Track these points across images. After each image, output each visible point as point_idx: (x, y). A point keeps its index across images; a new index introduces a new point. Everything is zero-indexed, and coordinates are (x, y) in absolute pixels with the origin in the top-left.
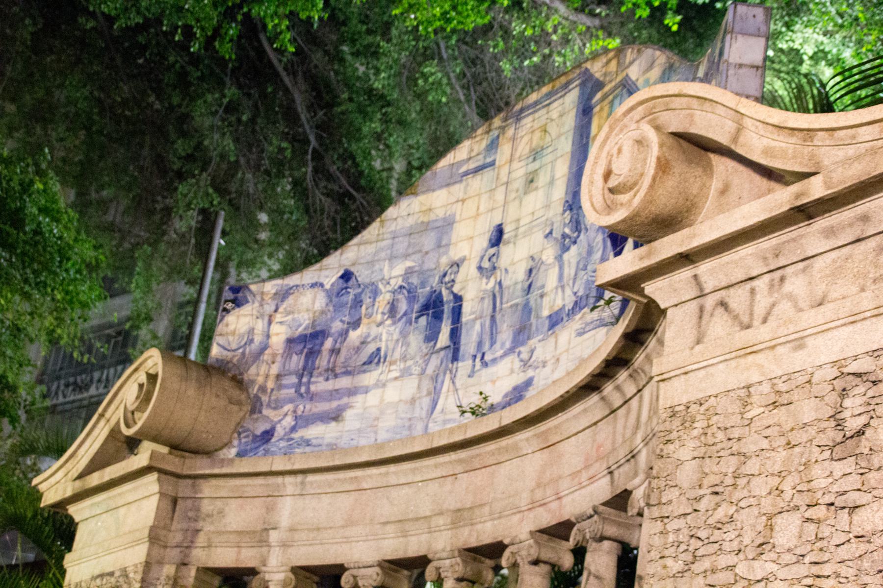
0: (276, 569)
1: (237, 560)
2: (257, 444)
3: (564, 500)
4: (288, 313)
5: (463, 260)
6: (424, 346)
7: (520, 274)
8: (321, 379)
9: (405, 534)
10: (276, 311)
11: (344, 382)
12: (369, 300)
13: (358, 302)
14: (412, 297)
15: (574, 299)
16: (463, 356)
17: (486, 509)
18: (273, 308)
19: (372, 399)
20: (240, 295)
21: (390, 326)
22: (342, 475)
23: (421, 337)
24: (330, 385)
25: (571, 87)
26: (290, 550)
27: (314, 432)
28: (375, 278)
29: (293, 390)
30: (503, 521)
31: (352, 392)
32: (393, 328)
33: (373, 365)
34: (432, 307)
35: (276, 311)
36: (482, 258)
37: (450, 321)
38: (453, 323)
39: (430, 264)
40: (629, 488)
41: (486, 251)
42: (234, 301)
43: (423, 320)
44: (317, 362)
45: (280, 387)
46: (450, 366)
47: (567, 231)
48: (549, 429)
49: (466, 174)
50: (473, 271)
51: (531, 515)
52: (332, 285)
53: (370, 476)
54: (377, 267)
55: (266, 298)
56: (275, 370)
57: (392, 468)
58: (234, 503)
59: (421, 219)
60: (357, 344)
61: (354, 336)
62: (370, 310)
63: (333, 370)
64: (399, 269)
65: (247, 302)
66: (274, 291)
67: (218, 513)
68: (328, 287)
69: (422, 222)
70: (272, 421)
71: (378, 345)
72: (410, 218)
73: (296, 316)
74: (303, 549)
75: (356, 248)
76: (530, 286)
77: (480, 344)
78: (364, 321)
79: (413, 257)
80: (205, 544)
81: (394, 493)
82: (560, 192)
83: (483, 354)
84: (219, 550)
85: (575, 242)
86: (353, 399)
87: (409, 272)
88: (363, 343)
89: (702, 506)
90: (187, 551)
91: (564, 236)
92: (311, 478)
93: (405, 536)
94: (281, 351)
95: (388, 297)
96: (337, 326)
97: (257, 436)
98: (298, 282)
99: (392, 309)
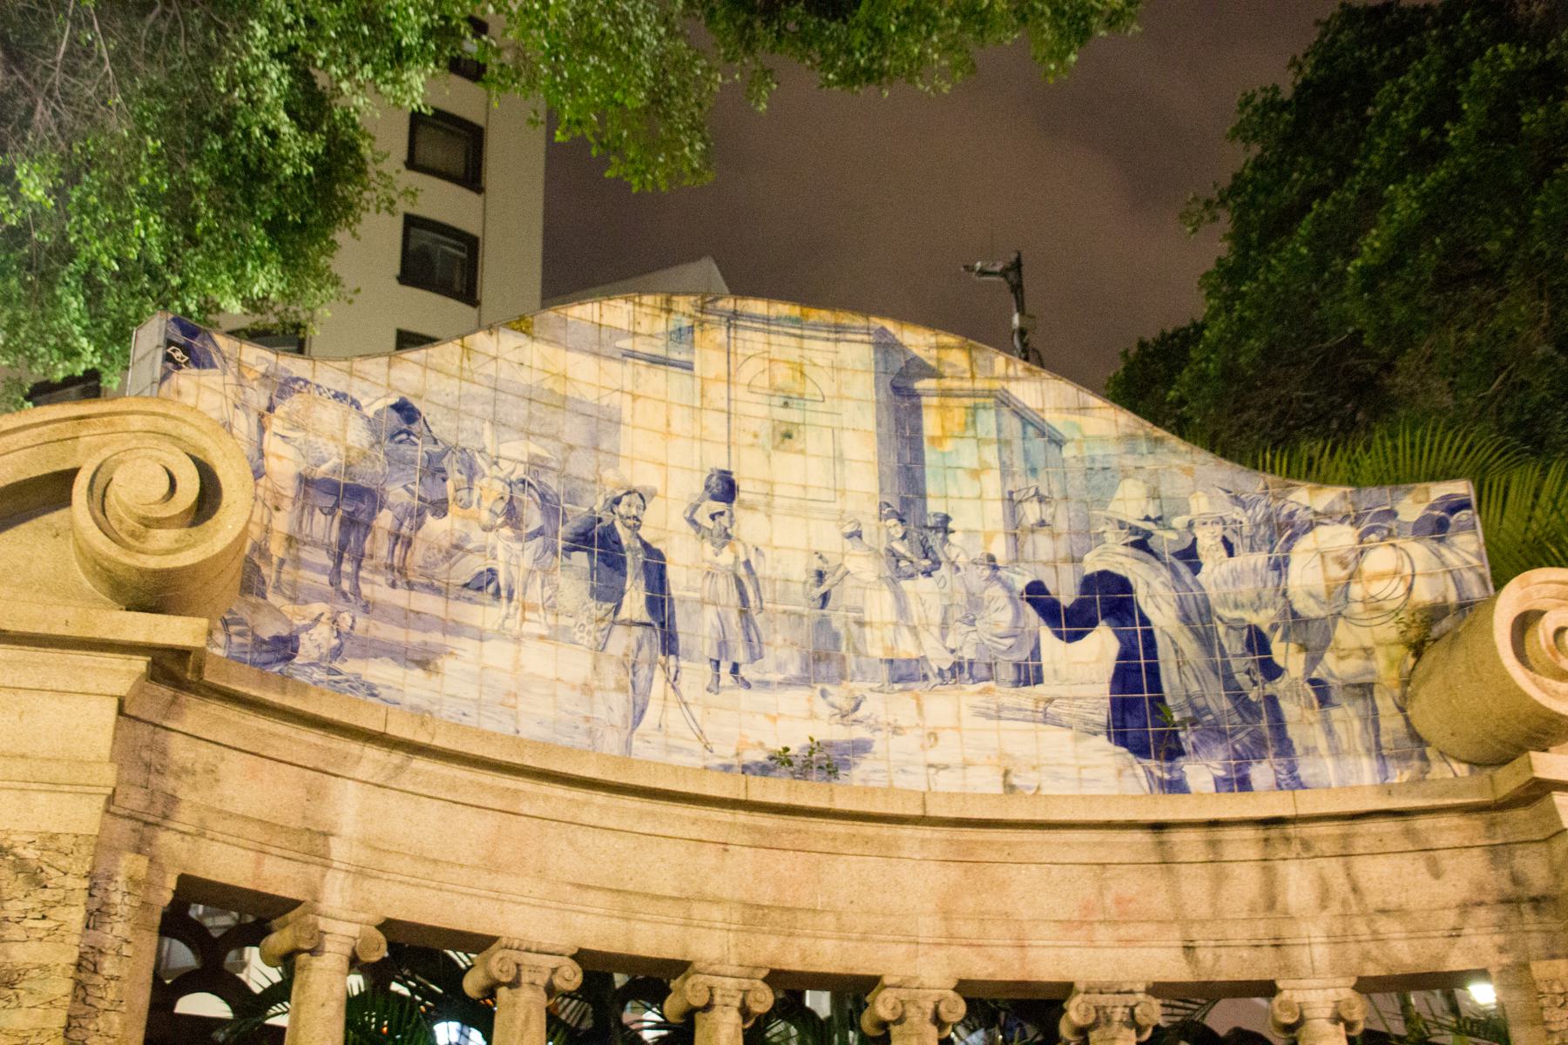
0: (346, 915)
1: (257, 876)
2: (265, 657)
3: (1032, 953)
4: (297, 427)
6: (592, 604)
7: (798, 569)
8: (380, 579)
9: (628, 916)
10: (271, 409)
11: (428, 603)
12: (458, 476)
14: (549, 505)
15: (952, 658)
16: (689, 652)
17: (829, 919)
18: (265, 403)
19: (497, 654)
20: (197, 343)
21: (508, 538)
22: (487, 778)
23: (584, 586)
25: (849, 336)
26: (367, 884)
27: (380, 672)
28: (465, 440)
29: (325, 579)
30: (866, 946)
31: (452, 628)
32: (517, 546)
33: (486, 596)
34: (600, 545)
35: (271, 409)
36: (695, 508)
37: (642, 583)
38: (649, 586)
39: (581, 465)
40: (1280, 985)
41: (702, 500)
42: (187, 349)
43: (581, 559)
44: (367, 544)
45: (298, 563)
46: (661, 658)
47: (900, 548)
48: (992, 843)
49: (631, 354)
51: (940, 953)
52: (377, 413)
53: (547, 798)
54: (467, 423)
55: (250, 376)
57: (600, 798)
58: (235, 761)
59: (548, 384)
60: (446, 544)
61: (435, 527)
62: (464, 494)
63: (402, 570)
65: (213, 366)
66: (261, 369)
67: (207, 772)
68: (370, 413)
69: (551, 391)
70: (290, 623)
71: (490, 564)
72: (525, 373)
73: (312, 438)
74: (396, 890)
75: (419, 370)
76: (825, 597)
77: (723, 645)
78: (453, 508)
79: (544, 441)
80: (193, 830)
81: (584, 838)
83: (735, 668)
84: (216, 847)
85: (928, 573)
86: (451, 641)
87: (536, 464)
88: (457, 547)
90: (147, 831)
91: (896, 557)
92: (420, 763)
93: (628, 919)
94: (291, 493)
95: (499, 487)
96: (398, 494)
97: (264, 642)
98: (308, 376)
99: (512, 514)
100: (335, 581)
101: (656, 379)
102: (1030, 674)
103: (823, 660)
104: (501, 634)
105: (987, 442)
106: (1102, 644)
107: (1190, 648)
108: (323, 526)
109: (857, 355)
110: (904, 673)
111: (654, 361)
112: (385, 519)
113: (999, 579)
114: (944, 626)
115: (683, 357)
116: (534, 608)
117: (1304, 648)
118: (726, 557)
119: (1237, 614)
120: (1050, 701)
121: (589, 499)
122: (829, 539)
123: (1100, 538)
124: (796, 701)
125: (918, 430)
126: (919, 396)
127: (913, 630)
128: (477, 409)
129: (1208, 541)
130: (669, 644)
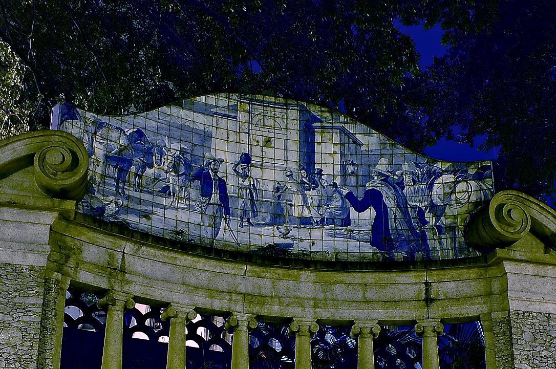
5: (222, 161)
7: (270, 187)
11: (146, 197)
13: (148, 153)
14: (188, 166)
24: (137, 195)
28: (159, 142)
32: (177, 178)
39: (198, 152)
43: (198, 183)
50: (230, 170)
56: (99, 170)
64: (176, 146)
76: (279, 196)
77: (244, 212)
79: (185, 143)
82: (294, 156)
85: (314, 189)
87: (182, 151)
89: (538, 349)
91: (303, 183)
97: (94, 209)
99: (175, 168)
100: (117, 190)
101: (223, 123)
102: (346, 222)
103: (278, 217)
104: (171, 207)
105: (336, 144)
106: (369, 214)
107: (399, 215)
108: (112, 171)
109: (294, 114)
110: (305, 222)
111: (224, 116)
112: (133, 169)
113: (338, 191)
114: (319, 206)
115: (233, 115)
116: (182, 199)
117: (435, 215)
118: (246, 183)
119: (414, 204)
120: (352, 231)
121: (201, 162)
122: (280, 177)
123: (371, 178)
124: (268, 230)
125: (313, 141)
126: (314, 129)
127: (308, 207)
128: (164, 132)
129: (407, 179)
130: (227, 212)
